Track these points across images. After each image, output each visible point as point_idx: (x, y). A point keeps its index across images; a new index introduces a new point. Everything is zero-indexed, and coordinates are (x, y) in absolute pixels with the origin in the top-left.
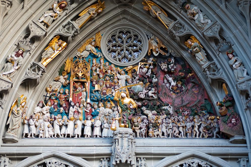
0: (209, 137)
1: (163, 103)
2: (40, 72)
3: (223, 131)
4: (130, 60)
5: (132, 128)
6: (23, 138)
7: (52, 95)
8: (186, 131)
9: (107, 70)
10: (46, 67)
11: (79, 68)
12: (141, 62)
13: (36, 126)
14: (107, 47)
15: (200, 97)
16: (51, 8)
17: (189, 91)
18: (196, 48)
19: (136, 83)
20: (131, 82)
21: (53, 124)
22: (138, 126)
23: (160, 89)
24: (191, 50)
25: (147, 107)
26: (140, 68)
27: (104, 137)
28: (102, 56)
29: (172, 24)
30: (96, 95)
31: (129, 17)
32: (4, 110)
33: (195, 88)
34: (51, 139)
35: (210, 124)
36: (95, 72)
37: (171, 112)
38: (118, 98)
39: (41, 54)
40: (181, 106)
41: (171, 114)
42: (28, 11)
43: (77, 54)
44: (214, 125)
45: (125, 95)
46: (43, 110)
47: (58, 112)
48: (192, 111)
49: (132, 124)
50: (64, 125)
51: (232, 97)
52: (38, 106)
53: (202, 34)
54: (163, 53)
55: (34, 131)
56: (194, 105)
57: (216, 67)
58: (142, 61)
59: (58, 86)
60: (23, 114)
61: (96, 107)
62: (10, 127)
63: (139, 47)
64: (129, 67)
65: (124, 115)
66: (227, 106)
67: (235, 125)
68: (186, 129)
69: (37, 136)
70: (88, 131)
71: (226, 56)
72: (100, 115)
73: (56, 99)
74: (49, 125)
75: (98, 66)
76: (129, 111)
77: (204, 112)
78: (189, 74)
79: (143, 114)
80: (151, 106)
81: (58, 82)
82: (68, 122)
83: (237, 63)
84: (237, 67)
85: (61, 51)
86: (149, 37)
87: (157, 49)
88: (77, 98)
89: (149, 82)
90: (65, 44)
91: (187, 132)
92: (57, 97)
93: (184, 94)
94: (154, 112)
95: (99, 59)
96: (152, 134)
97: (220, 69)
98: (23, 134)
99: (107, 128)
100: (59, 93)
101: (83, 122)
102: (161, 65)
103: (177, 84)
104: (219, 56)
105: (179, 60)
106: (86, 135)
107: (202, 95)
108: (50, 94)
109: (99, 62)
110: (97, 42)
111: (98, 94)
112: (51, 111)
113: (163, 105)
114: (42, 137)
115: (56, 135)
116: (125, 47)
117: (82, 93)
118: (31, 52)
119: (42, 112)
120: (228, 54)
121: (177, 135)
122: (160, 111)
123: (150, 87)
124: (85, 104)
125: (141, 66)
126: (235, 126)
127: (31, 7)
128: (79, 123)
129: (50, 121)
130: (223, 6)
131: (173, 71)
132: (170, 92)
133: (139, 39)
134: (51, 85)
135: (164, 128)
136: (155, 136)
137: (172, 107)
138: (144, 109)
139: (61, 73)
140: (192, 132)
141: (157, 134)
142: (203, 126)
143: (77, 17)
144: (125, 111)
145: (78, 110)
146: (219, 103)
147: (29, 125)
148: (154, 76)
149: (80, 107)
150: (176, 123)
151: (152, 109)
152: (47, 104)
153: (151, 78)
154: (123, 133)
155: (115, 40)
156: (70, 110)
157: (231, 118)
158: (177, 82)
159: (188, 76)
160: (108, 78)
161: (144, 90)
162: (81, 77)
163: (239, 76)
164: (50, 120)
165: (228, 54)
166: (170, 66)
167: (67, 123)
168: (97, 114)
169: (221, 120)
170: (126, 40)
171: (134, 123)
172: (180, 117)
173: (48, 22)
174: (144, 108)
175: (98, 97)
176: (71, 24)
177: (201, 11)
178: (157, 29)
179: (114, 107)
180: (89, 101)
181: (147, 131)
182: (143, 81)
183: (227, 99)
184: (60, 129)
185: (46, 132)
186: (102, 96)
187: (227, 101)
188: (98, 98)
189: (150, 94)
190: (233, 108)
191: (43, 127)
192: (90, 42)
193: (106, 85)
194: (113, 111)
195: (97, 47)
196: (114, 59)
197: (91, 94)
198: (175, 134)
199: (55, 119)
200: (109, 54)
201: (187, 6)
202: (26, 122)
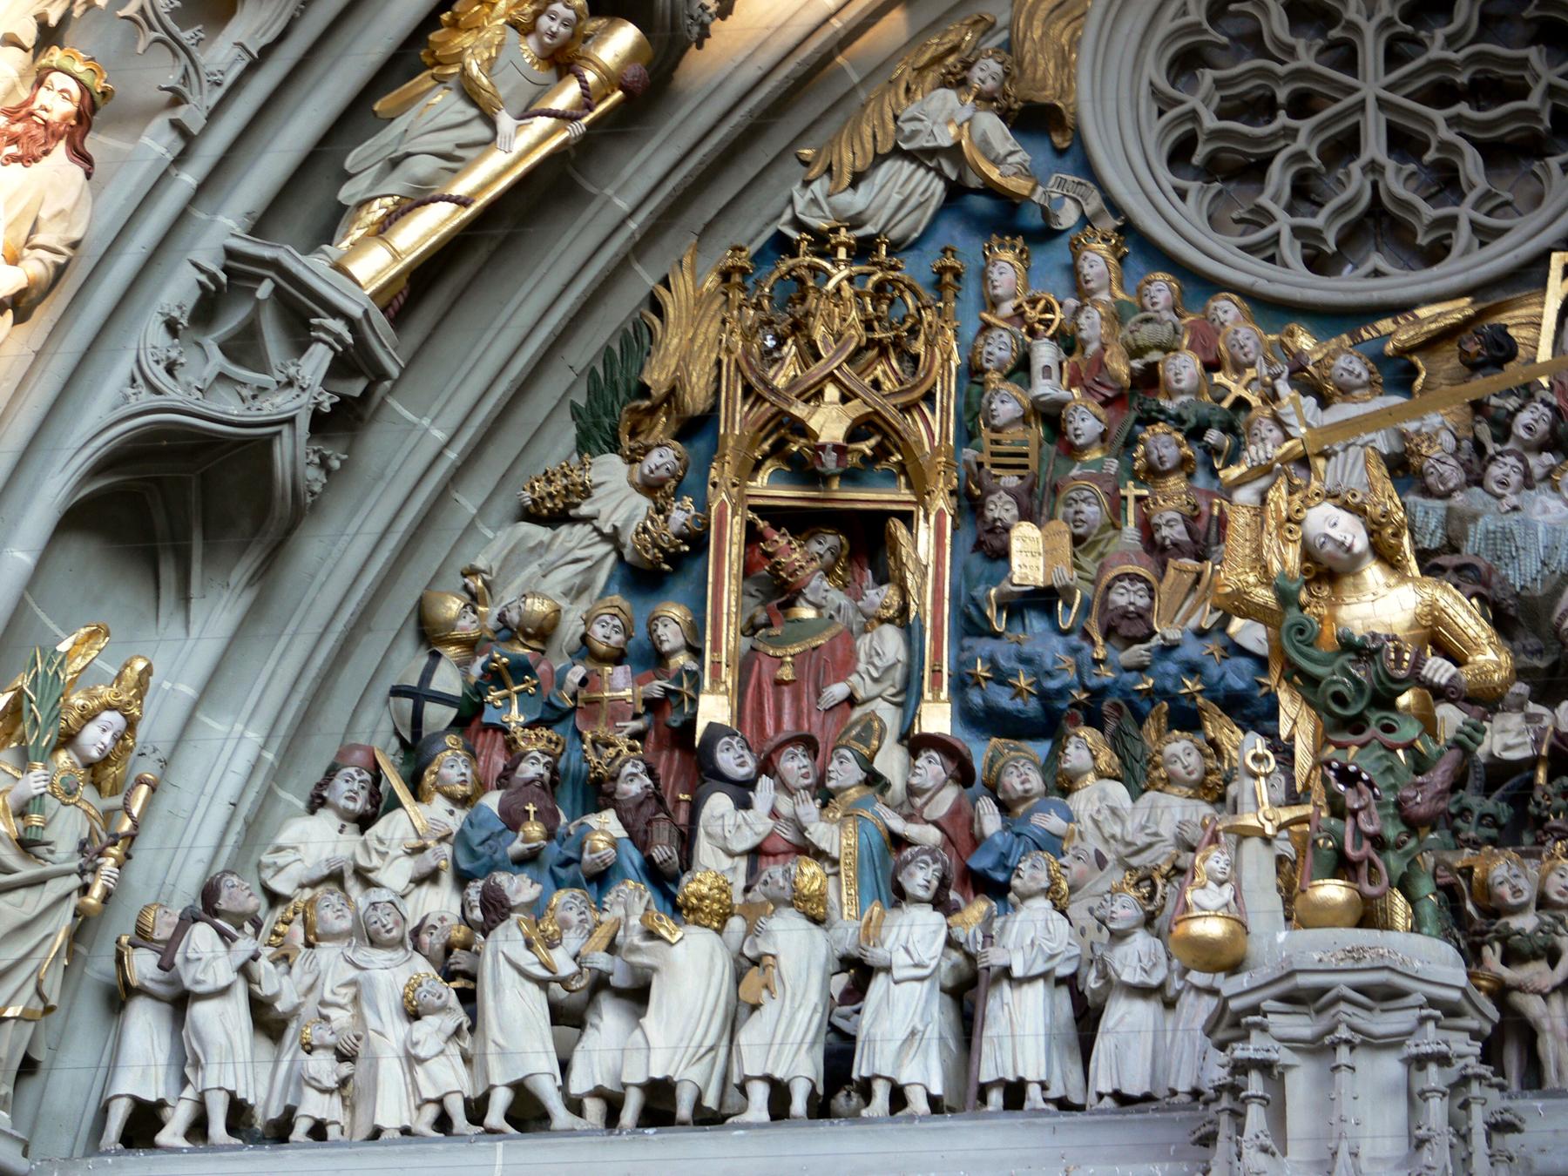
2: (318, 359)
7: (494, 677)
9: (1155, 356)
11: (812, 345)
14: (1161, 113)
19: (1515, 479)
20: (1452, 473)
21: (472, 977)
27: (1108, 1103)
28: (1097, 215)
30: (1027, 649)
34: (439, 1147)
36: (1008, 388)
43: (800, 204)
45: (1350, 531)
46: (374, 843)
47: (561, 872)
50: (619, 993)
52: (317, 803)
59: (566, 575)
61: (1023, 777)
63: (1552, 90)
64: (1423, 312)
72: (1076, 867)
74: (413, 986)
75: (1047, 323)
81: (564, 530)
82: (651, 935)
85: (578, 128)
88: (797, 699)
92: (549, 704)
95: (1058, 252)
98: (103, 1112)
99: (1142, 992)
106: (881, 1092)
108: (466, 674)
110: (1034, 62)
111: (1057, 642)
112: (473, 854)
114: (333, 1132)
115: (501, 1099)
116: (1371, 105)
117: (863, 644)
118: (192, 116)
124: (891, 761)
129: (448, 949)
134: (481, 563)
144: (1356, 725)
145: (801, 830)
147: (180, 1002)
152: (429, 779)
154: (1342, 983)
156: (701, 832)
162: (837, 448)
170: (1388, 23)
171: (1495, 910)
175: (1049, 674)
185: (374, 1061)
186: (1100, 653)
191: (340, 1017)
192: (951, 60)
196: (1249, 249)
197: (967, 642)
199: (496, 908)
200: (1182, 194)
202: (143, 965)
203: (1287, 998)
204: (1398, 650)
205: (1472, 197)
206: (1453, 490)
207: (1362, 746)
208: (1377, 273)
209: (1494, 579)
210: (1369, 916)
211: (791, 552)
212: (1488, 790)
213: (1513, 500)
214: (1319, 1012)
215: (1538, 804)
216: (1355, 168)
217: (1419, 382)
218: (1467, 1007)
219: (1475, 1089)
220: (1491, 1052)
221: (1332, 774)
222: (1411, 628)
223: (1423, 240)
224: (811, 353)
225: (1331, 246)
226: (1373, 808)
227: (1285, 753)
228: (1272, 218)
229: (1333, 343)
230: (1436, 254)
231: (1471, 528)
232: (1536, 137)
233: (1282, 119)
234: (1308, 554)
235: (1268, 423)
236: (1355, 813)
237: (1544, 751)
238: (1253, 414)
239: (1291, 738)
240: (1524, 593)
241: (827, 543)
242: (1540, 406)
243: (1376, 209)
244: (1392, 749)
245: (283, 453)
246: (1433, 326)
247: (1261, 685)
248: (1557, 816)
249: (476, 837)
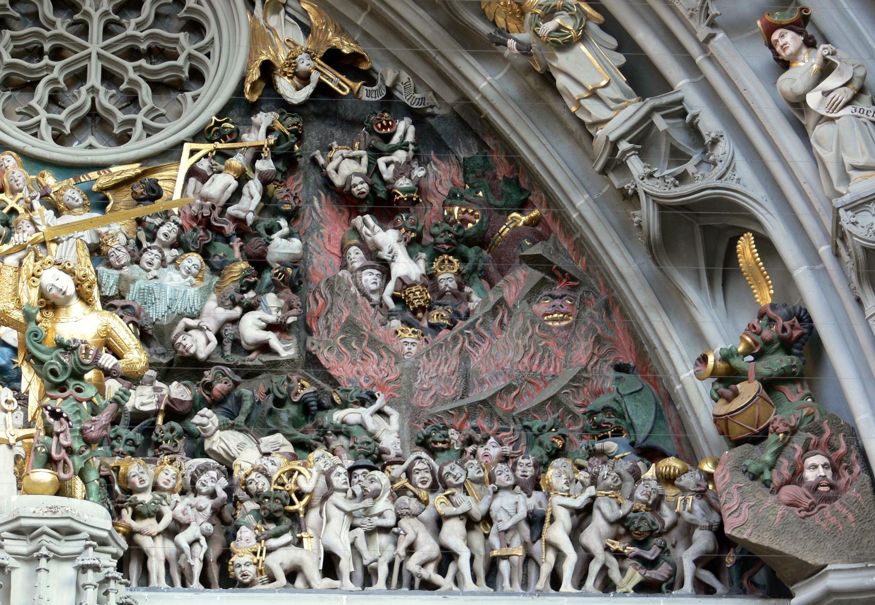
0: (646, 588)
1: (334, 383)
3: (745, 536)
8: (489, 548)
17: (510, 317)
18: (557, 21)
19: (157, 261)
22: (159, 517)
23: (321, 301)
33: (553, 297)
35: (656, 505)
40: (460, 409)
44: (679, 508)
45: (67, 285)
51: (804, 317)
56: (545, 398)
57: (693, 130)
58: (199, 136)
63: (190, 57)
64: (114, 169)
66: (766, 372)
67: (828, 499)
68: (486, 536)
78: (514, 214)
80: (256, 404)
83: (831, 82)
84: (834, 107)
87: (304, 55)
91: (495, 553)
93: (478, 333)
96: (257, 564)
97: (715, 142)
102: (331, 159)
103: (431, 277)
104: (711, 58)
107: (598, 340)
113: (338, 402)
116: (94, 57)
120: (770, 28)
121: (430, 573)
123: (251, 286)
125: (199, 160)
126: (828, 506)
131: (404, 191)
132: (383, 324)
133: (191, 10)
135: (339, 522)
136: (272, 579)
137: (395, 416)
138: (204, 420)
141: (287, 565)
142: (609, 515)
144: (62, 387)
146: (711, 359)
150: (423, 495)
153: (264, 232)
154: (45, 525)
161: (212, 304)
163: (848, 160)
166: (388, 164)
169: (731, 462)
170: (106, 13)
171: (129, 491)
183: (767, 334)
187: (768, 343)
190: (807, 391)
196: (24, 129)
198: (413, 565)
203: (16, 531)
204: (87, 349)
205: (144, 110)
206: (123, 266)
207: (65, 399)
208: (91, 146)
209: (142, 314)
210: (62, 490)
212: (132, 425)
213: (154, 273)
214: (32, 539)
215: (157, 435)
216: (83, 89)
217: (109, 207)
218: (111, 541)
219: (112, 585)
220: (122, 565)
221: (47, 412)
222: (95, 337)
223: (117, 131)
225: (67, 131)
226: (68, 432)
227: (23, 400)
228: (37, 113)
229: (65, 182)
230: (123, 139)
231: (132, 286)
232: (180, 81)
233: (46, 60)
234: (42, 295)
235: (27, 223)
236: (58, 434)
237: (162, 408)
238: (19, 217)
239: (27, 392)
240: (157, 323)
242: (173, 224)
243: (93, 113)
244: (80, 401)
246: (119, 177)
247: (14, 363)
248: (166, 442)
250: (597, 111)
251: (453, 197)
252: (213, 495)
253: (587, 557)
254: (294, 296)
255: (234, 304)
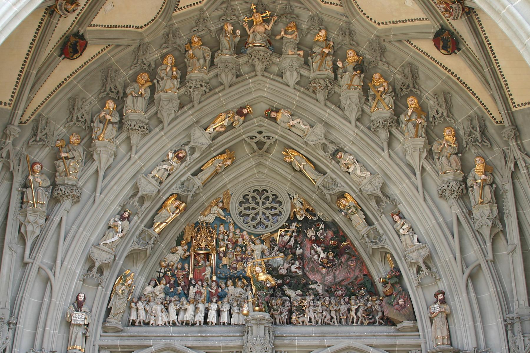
0: (369, 324)
2: (152, 241)
4: (267, 226)
5: (269, 312)
6: (129, 326)
10: (159, 234)
12: (281, 228)
13: (146, 311)
15: (357, 273)
16: (166, 158)
20: (268, 254)
22: (278, 311)
24: (346, 211)
25: (290, 286)
26: (281, 235)
29: (320, 180)
31: (266, 171)
32: (104, 290)
35: (371, 307)
37: (321, 292)
38: (252, 273)
39: (153, 218)
40: (334, 284)
41: (321, 294)
42: (137, 163)
44: (376, 307)
48: (348, 290)
49: (270, 308)
51: (400, 271)
53: (359, 191)
54: (309, 216)
55: (143, 317)
57: (378, 232)
58: (281, 228)
60: (129, 294)
61: (223, 286)
62: (112, 312)
64: (266, 235)
65: (259, 295)
67: (404, 308)
68: (339, 313)
69: (147, 324)
70: (212, 317)
71: (391, 219)
73: (172, 276)
74: (162, 309)
76: (266, 291)
77: (363, 291)
79: (284, 294)
83: (405, 227)
85: (179, 215)
86: (291, 196)
89: (292, 253)
90: (184, 205)
94: (299, 292)
95: (227, 225)
98: (129, 321)
100: (177, 268)
101: (207, 305)
103: (327, 257)
105: (331, 225)
106: (210, 322)
107: (360, 270)
109: (227, 228)
114: (154, 325)
117: (206, 268)
118: (140, 216)
119: (154, 293)
120: (393, 215)
122: (306, 290)
123: (293, 259)
127: (139, 158)
128: (201, 306)
130: (385, 154)
135: (311, 311)
136: (300, 323)
137: (321, 286)
139: (179, 243)
140: (347, 317)
141: (302, 321)
143: (200, 170)
148: (299, 246)
149: (203, 286)
150: (327, 306)
151: (295, 289)
155: (247, 200)
157: (398, 298)
158: (327, 254)
159: (342, 246)
160: (238, 249)
164: (163, 303)
165: (393, 215)
167: (186, 307)
168: (225, 296)
169: (385, 301)
171: (272, 306)
172: (332, 298)
173: (162, 176)
174: (285, 288)
176: (192, 180)
177: (358, 162)
178: (301, 186)
179: (247, 286)
180: (214, 278)
181: (289, 315)
182: (284, 253)
183: (392, 275)
184: (177, 315)
187: (392, 276)
188: (226, 275)
189: (293, 268)
191: (154, 312)
193: (236, 258)
194: (246, 291)
195: (224, 210)
198: (326, 320)
199: (170, 301)
201: (339, 155)
202: (133, 305)
208: (260, 229)
211: (198, 258)
224: (201, 237)
241: (202, 256)
245: (148, 251)
249: (166, 289)
250: (359, 228)
251: (332, 239)
252: (288, 306)
253: (358, 318)
254: (301, 262)
255: (290, 263)
